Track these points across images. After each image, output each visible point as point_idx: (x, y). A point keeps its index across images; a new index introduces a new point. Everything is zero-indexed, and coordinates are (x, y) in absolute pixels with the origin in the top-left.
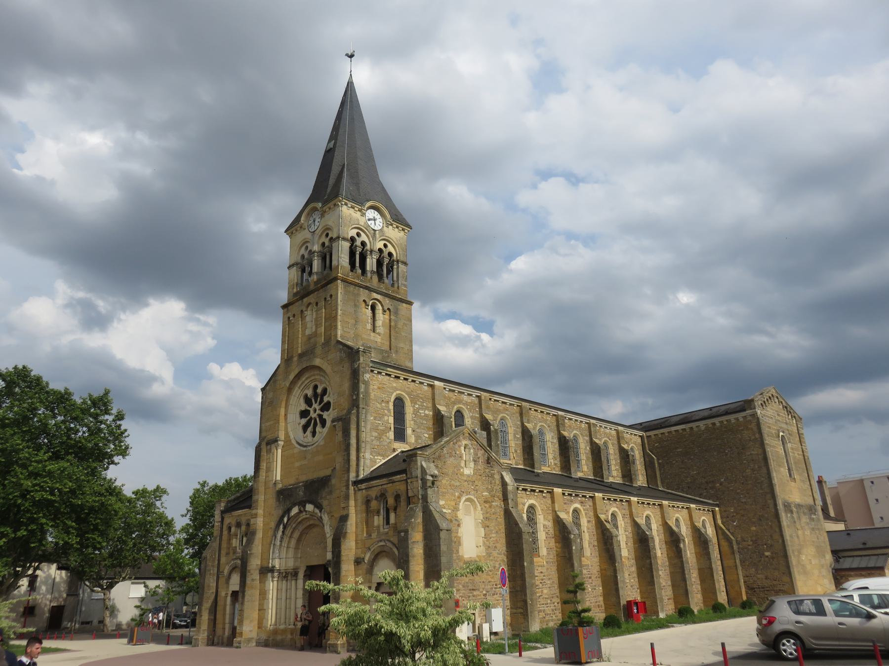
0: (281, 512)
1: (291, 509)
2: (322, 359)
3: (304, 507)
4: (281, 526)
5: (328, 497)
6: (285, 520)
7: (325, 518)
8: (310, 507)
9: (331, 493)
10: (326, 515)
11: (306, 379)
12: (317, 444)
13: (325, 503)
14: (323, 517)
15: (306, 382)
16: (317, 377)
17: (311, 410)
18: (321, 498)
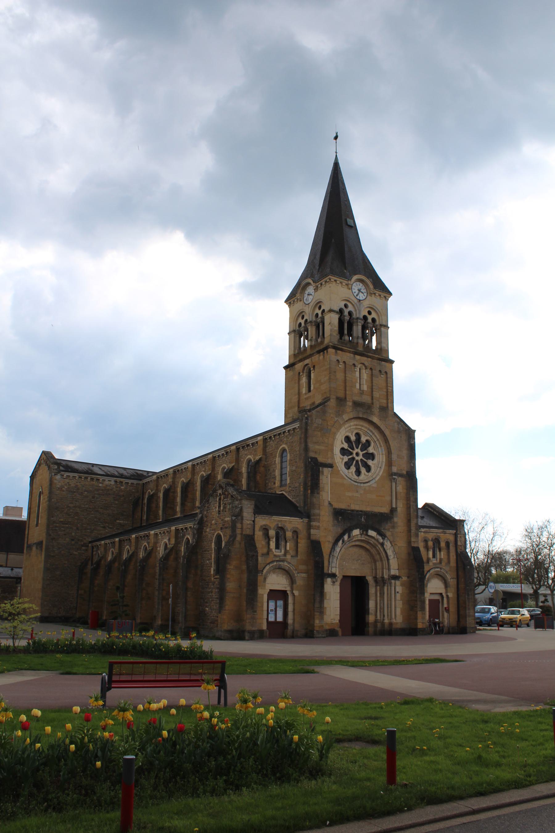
0: (340, 530)
1: (352, 530)
2: (380, 420)
3: (367, 531)
4: (341, 541)
5: (391, 530)
6: (346, 537)
7: (388, 545)
8: (372, 533)
9: (393, 527)
10: (389, 543)
11: (355, 425)
12: (368, 484)
13: (388, 534)
14: (386, 543)
15: (352, 427)
16: (363, 428)
17: (361, 453)
18: (384, 529)
